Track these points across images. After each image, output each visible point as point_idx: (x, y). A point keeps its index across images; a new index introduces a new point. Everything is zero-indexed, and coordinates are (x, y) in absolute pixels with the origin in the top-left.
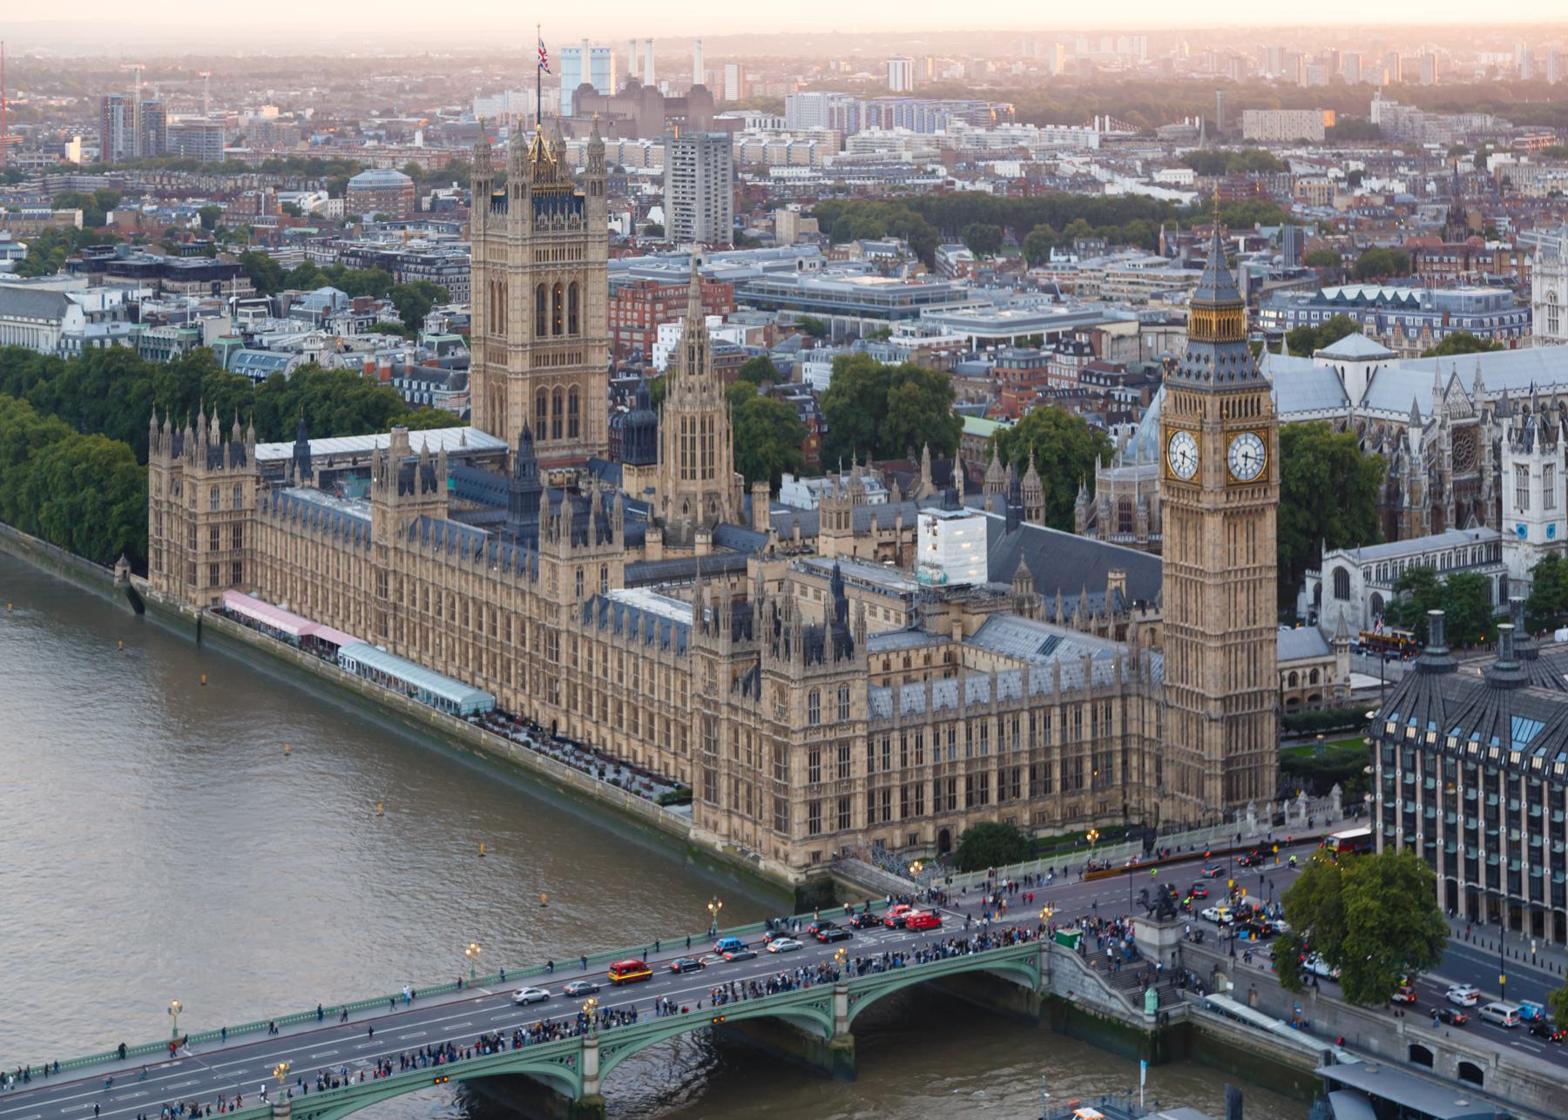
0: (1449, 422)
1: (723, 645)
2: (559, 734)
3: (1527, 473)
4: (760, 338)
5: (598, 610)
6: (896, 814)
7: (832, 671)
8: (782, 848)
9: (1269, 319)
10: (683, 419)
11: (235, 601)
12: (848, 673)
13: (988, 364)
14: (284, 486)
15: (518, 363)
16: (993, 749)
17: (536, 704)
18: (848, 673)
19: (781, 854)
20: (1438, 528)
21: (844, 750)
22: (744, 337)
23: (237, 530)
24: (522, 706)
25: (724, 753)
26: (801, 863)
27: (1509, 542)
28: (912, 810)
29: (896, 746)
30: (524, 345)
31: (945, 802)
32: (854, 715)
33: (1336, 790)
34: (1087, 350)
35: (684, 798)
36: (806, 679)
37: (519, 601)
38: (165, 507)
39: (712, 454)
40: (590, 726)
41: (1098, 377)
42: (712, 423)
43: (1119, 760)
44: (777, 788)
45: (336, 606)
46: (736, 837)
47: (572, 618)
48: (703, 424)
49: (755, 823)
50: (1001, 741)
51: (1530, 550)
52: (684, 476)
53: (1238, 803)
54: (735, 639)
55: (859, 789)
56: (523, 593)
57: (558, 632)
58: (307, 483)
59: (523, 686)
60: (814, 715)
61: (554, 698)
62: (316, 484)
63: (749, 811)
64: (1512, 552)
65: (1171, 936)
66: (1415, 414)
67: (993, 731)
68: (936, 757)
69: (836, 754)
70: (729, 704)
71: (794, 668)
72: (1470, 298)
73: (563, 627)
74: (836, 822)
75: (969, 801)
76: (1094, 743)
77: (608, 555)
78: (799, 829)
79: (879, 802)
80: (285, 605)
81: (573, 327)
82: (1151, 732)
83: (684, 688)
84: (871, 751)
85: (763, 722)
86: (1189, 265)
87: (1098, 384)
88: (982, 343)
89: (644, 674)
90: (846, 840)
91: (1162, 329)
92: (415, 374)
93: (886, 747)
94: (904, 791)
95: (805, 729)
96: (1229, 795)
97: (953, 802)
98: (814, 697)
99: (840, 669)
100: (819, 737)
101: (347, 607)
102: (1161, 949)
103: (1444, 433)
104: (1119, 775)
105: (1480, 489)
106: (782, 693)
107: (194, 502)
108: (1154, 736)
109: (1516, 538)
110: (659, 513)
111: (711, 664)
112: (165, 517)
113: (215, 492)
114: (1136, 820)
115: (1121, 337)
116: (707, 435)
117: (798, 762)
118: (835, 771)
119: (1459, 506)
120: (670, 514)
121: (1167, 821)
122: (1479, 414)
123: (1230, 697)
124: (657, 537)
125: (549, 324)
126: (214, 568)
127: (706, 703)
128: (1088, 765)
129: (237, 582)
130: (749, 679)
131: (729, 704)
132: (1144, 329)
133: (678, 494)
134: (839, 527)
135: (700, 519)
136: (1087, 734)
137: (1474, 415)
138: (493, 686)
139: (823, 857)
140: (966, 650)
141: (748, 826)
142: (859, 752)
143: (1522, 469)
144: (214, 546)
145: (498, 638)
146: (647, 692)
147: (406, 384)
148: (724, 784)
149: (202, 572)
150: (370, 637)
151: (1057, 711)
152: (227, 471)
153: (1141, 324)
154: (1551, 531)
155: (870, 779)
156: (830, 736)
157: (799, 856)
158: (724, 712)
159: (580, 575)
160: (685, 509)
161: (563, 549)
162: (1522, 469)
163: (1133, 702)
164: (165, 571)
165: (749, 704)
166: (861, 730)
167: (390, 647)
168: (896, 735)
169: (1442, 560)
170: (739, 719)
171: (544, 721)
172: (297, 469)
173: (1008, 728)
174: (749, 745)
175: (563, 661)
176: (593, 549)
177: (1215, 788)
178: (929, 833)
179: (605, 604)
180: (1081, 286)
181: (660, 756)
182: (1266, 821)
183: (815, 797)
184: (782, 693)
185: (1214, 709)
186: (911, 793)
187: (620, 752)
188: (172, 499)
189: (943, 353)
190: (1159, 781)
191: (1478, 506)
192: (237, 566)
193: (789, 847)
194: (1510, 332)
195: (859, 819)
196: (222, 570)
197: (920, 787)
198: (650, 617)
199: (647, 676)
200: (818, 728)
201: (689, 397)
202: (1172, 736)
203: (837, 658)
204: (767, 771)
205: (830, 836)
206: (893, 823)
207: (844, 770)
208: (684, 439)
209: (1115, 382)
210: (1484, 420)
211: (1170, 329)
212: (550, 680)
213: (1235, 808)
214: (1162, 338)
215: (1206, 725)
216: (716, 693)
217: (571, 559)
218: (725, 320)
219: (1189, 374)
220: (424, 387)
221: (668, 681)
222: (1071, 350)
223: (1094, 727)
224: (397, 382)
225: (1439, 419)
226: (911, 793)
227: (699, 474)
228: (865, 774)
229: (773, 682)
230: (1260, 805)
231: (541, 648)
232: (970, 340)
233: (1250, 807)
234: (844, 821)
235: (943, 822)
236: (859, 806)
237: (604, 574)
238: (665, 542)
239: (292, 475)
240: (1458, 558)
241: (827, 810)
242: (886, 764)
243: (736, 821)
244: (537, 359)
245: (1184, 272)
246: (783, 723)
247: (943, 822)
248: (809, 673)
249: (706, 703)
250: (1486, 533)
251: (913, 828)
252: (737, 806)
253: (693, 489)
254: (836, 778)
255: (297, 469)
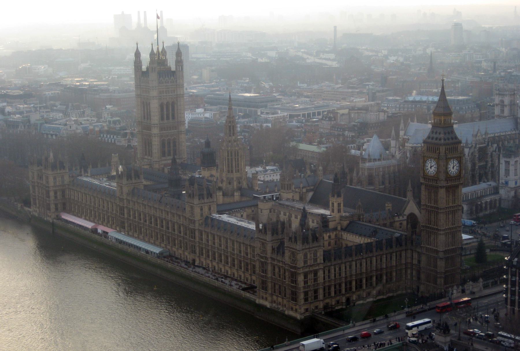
0: (478, 146)
1: (269, 237)
2: (196, 264)
3: (509, 164)
4: (218, 116)
5: (208, 221)
6: (333, 294)
7: (311, 246)
8: (294, 307)
9: (385, 107)
10: (228, 152)
11: (67, 217)
12: (317, 247)
13: (297, 124)
14: (78, 176)
15: (155, 131)
16: (364, 270)
17: (186, 254)
18: (317, 247)
19: (294, 309)
20: (474, 183)
21: (316, 273)
22: (212, 115)
23: (63, 192)
24: (181, 254)
25: (269, 275)
26: (302, 312)
27: (501, 187)
28: (338, 292)
29: (332, 271)
30: (157, 124)
31: (349, 289)
32: (319, 261)
33: (481, 280)
34: (333, 119)
35: (251, 288)
36: (303, 249)
37: (178, 218)
38: (36, 184)
39: (238, 164)
40: (209, 262)
41: (338, 128)
42: (238, 153)
43: (404, 271)
44: (292, 287)
45: (104, 218)
46: (275, 302)
47: (199, 224)
48: (235, 153)
49: (283, 298)
50: (366, 267)
51: (509, 189)
52: (229, 172)
53: (448, 286)
54: (273, 234)
55: (321, 286)
56: (179, 216)
57: (195, 230)
58: (86, 174)
59: (181, 247)
60: (305, 262)
61: (194, 252)
62: (89, 175)
63: (280, 294)
64: (503, 190)
65: (448, 339)
66: (467, 143)
67: (364, 264)
68: (346, 274)
69: (313, 275)
70: (271, 258)
71: (299, 246)
72: (458, 100)
73: (197, 228)
74: (313, 298)
75: (356, 288)
76: (396, 266)
77: (211, 202)
78: (302, 302)
79: (327, 291)
80: (83, 218)
81: (173, 118)
82: (415, 262)
83: (246, 249)
84: (324, 273)
85: (285, 264)
86: (349, 88)
87: (337, 131)
88: (291, 116)
89: (230, 244)
90: (317, 304)
91: (356, 111)
92: (108, 132)
93: (329, 271)
94: (335, 286)
95: (303, 267)
96: (446, 283)
97: (351, 289)
98: (305, 255)
99: (314, 246)
100: (307, 270)
101: (108, 218)
102: (445, 343)
103: (476, 150)
104: (404, 276)
105: (486, 168)
106: (293, 254)
107: (47, 182)
108: (416, 263)
109: (504, 185)
110: (220, 185)
111: (263, 244)
112: (36, 188)
113: (55, 178)
114: (409, 291)
115: (343, 114)
116: (237, 157)
117: (301, 279)
118: (313, 281)
119: (480, 174)
120: (224, 185)
121: (422, 292)
122: (486, 143)
123: (446, 250)
124: (221, 193)
125: (165, 116)
126: (56, 205)
127: (262, 257)
128: (394, 274)
129: (65, 210)
130: (278, 248)
131: (271, 258)
132: (350, 111)
133: (227, 178)
134: (288, 189)
135: (235, 187)
136: (394, 263)
137: (484, 143)
138: (168, 247)
139: (309, 310)
140: (343, 233)
141: (280, 300)
142: (321, 274)
143: (507, 163)
144: (56, 197)
145: (170, 231)
146: (231, 251)
147: (105, 136)
148: (270, 285)
149: (53, 207)
150: (118, 229)
151: (385, 256)
152: (59, 171)
153: (350, 110)
154: (516, 183)
155: (324, 282)
156: (311, 269)
157: (303, 311)
158: (269, 261)
159: (202, 209)
160: (230, 183)
161: (196, 201)
162: (507, 163)
163: (409, 251)
164: (38, 206)
165: (280, 258)
166: (321, 266)
167: (126, 233)
168: (333, 267)
169: (480, 193)
170: (276, 263)
171: (190, 259)
172: (82, 170)
173: (369, 262)
174: (280, 271)
175: (197, 239)
176: (206, 200)
177: (441, 281)
178: (344, 300)
179: (212, 219)
180: (315, 95)
181: (238, 273)
182: (459, 292)
183: (306, 290)
184: (293, 254)
185: (441, 255)
186: (337, 287)
187: (221, 271)
188: (39, 181)
189: (281, 120)
190: (419, 278)
191: (486, 174)
192: (64, 204)
193: (297, 307)
194: (471, 111)
195: (321, 296)
196: (59, 206)
197: (340, 285)
198: (232, 225)
199: (231, 245)
200: (307, 267)
201: (230, 144)
202: (423, 264)
203: (313, 241)
204: (287, 281)
205: (311, 303)
206: (332, 297)
207: (315, 280)
208: (228, 159)
209: (344, 130)
210: (488, 145)
211: (359, 111)
212: (192, 245)
213: (447, 288)
214: (356, 115)
215: (438, 260)
216: (266, 254)
217: (199, 204)
218: (205, 110)
219: (433, 138)
220: (112, 137)
221: (240, 247)
222: (327, 119)
223: (396, 261)
224: (102, 135)
225: (474, 145)
226: (337, 287)
227: (234, 171)
228: (322, 281)
229: (289, 250)
230: (458, 286)
231: (188, 235)
232: (287, 115)
233: (455, 287)
234: (316, 297)
235: (348, 295)
236: (321, 292)
237: (210, 209)
238: (224, 195)
239: (81, 172)
240: (485, 192)
241: (311, 294)
242: (329, 277)
243: (275, 298)
244: (161, 129)
245: (350, 90)
246: (294, 265)
247: (348, 295)
248: (304, 248)
249: (262, 257)
250: (493, 184)
251: (338, 298)
252: (275, 292)
253: (232, 176)
254: (313, 283)
255: (82, 170)
